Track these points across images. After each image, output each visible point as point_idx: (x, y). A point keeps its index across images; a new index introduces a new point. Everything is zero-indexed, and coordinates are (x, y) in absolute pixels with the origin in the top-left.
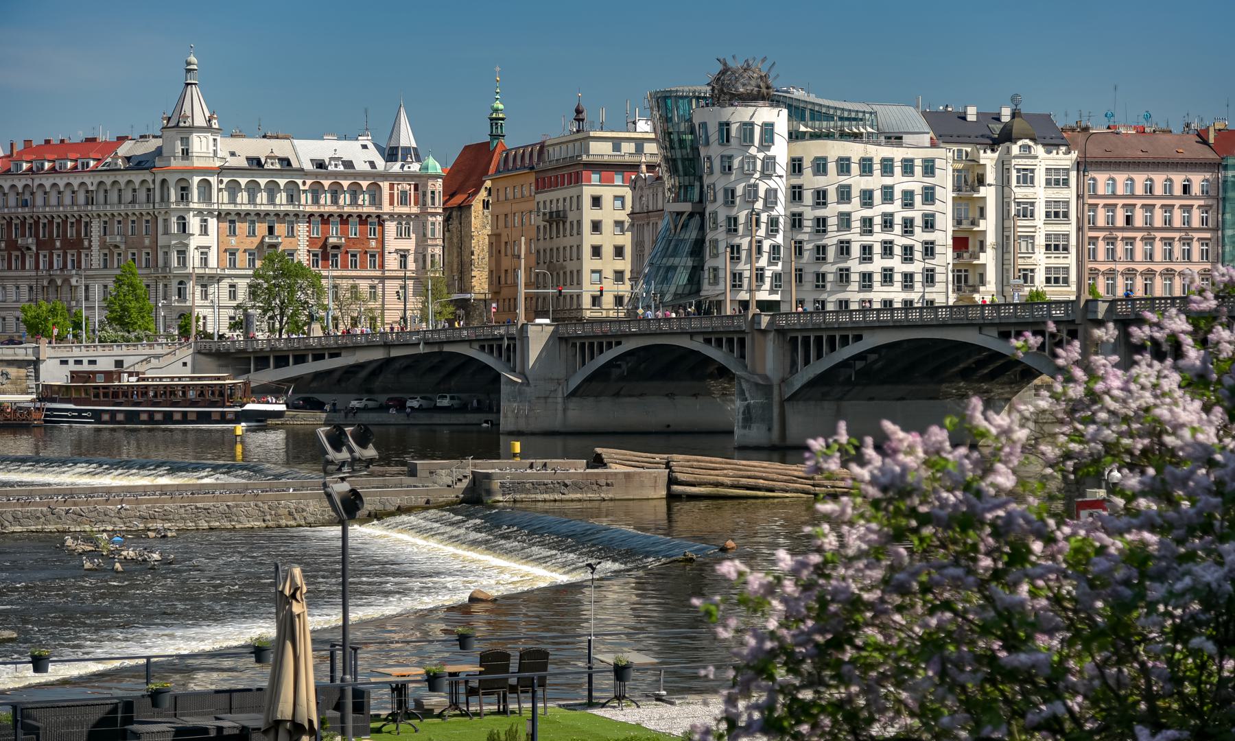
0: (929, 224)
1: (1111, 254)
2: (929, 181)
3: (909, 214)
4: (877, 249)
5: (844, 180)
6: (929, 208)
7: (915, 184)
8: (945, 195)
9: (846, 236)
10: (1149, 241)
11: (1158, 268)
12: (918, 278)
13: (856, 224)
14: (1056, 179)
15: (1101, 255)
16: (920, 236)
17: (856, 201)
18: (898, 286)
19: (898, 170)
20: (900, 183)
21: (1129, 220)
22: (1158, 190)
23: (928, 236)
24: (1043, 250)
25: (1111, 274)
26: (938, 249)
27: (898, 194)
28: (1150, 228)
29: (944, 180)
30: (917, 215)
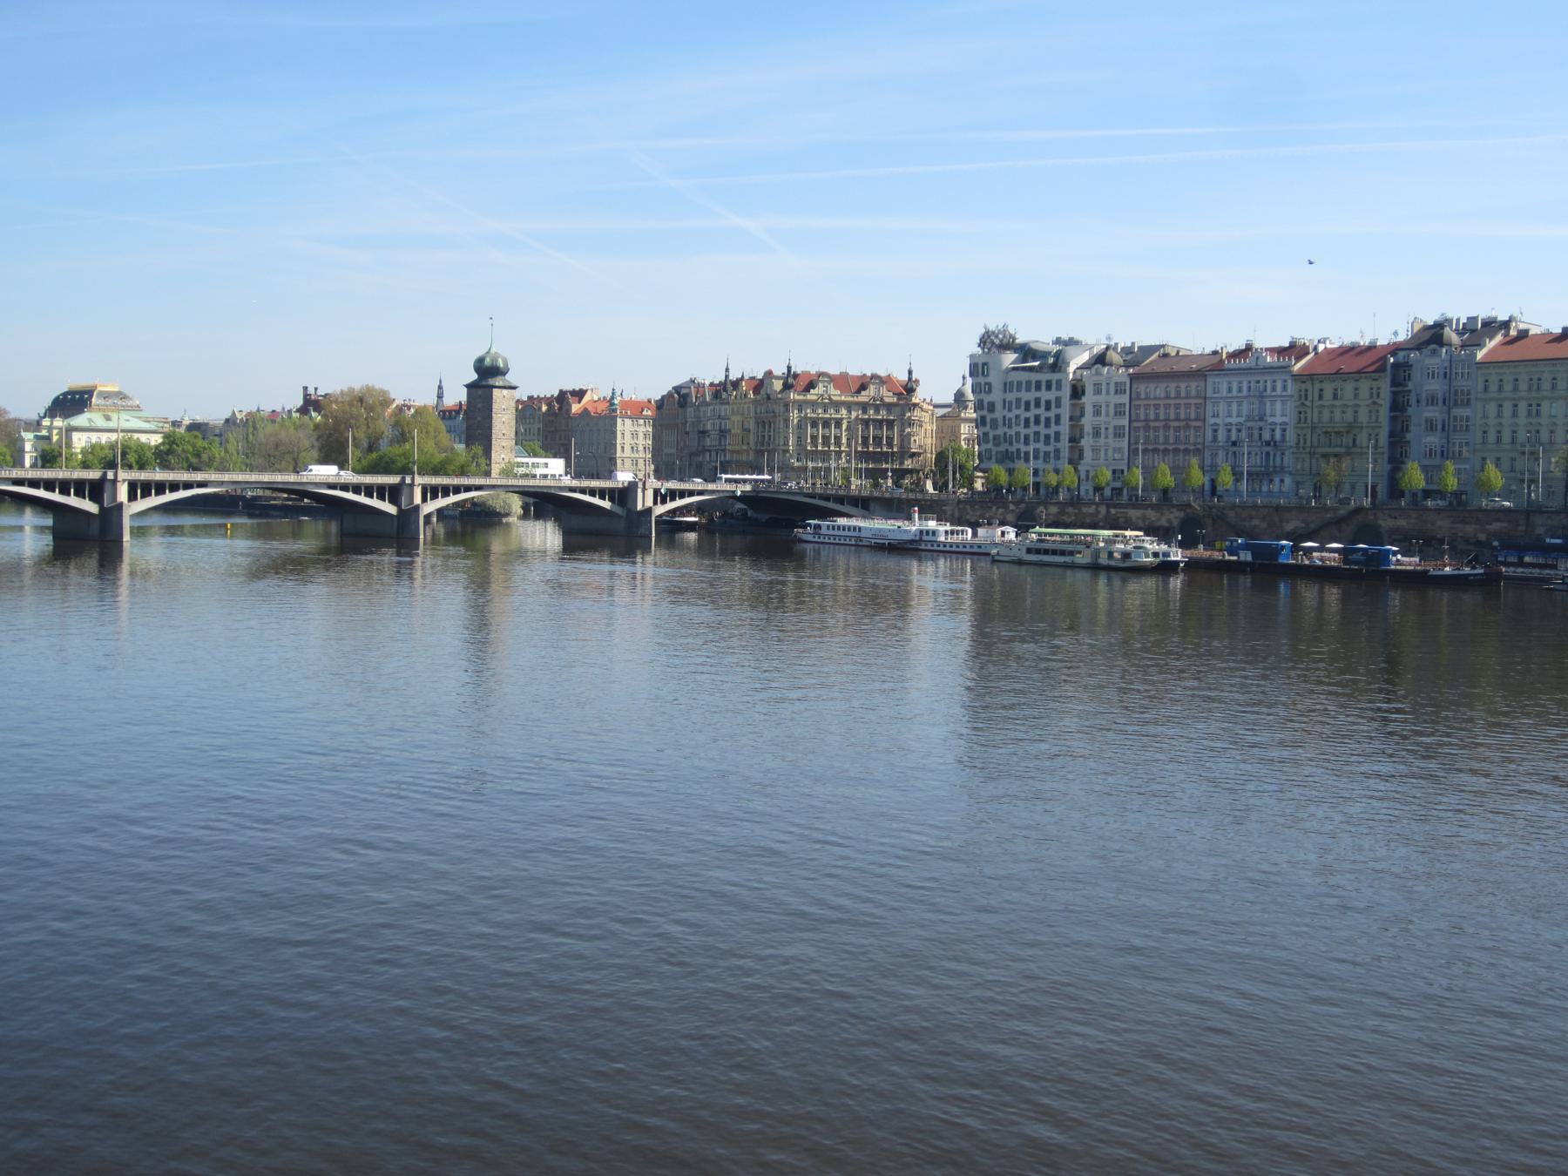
0: (1058, 418)
1: (1166, 438)
2: (1058, 394)
6: (1059, 411)
11: (1171, 448)
16: (1054, 428)
19: (1044, 387)
20: (1045, 395)
24: (1111, 436)
26: (1062, 437)
27: (1043, 403)
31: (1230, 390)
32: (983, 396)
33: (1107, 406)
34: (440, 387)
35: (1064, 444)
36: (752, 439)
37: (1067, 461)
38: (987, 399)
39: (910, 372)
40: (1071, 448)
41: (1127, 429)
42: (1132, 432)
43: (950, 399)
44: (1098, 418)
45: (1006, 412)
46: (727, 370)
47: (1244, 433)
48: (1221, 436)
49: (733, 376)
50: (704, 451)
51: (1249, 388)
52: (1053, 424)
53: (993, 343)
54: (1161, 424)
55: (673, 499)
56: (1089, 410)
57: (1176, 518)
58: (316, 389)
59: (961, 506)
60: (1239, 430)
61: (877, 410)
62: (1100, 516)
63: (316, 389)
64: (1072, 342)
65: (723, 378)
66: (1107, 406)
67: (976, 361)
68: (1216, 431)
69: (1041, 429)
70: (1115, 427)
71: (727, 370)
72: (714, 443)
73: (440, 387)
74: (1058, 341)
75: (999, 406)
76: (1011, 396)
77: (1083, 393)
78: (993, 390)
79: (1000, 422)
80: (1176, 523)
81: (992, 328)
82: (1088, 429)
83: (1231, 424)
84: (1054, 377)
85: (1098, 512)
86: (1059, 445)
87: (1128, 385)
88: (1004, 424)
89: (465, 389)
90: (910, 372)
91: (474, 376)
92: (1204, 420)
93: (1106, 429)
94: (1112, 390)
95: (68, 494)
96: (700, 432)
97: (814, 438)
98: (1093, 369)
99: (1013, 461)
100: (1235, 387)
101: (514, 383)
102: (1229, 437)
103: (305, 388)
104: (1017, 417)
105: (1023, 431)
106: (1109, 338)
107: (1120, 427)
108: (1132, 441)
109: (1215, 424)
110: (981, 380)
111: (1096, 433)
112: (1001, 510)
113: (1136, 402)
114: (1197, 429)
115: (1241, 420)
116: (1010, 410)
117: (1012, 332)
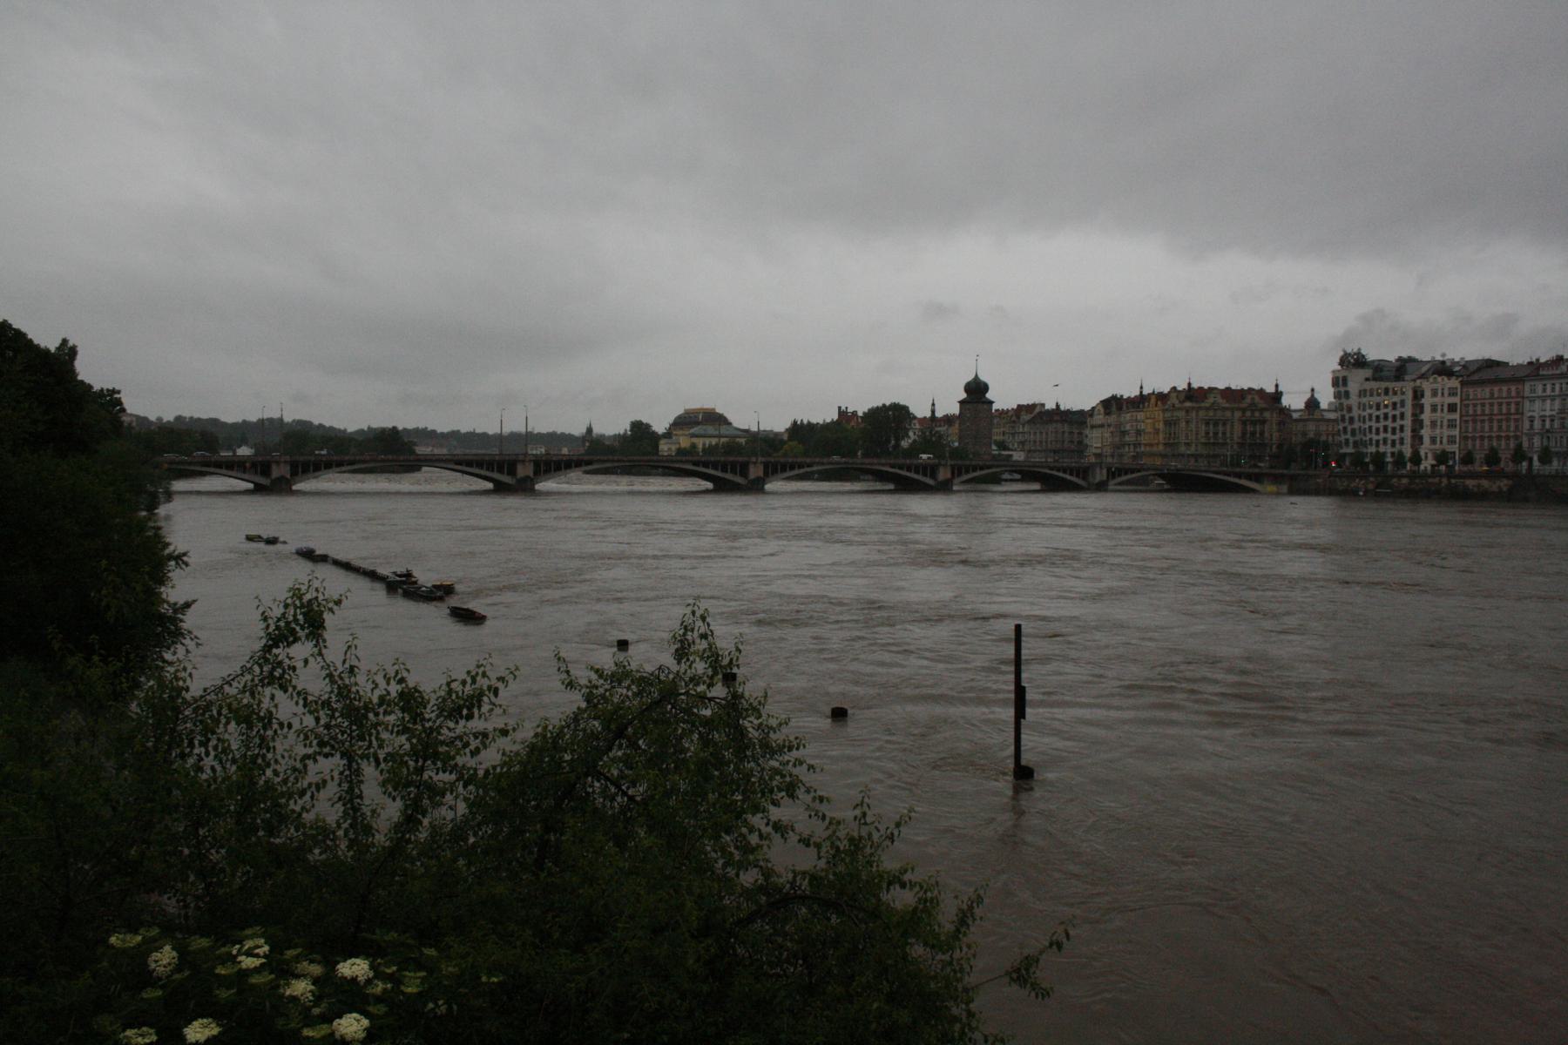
0: (1402, 416)
3: (1394, 413)
4: (1381, 430)
5: (1371, 399)
6: (1403, 410)
7: (1396, 399)
8: (1409, 403)
9: (1377, 425)
10: (1491, 421)
11: (1494, 435)
12: (1397, 442)
13: (1374, 418)
14: (1452, 393)
15: (1487, 428)
16: (1399, 422)
17: (1374, 408)
18: (1389, 446)
21: (1483, 411)
22: (1513, 394)
23: (1402, 423)
24: (1445, 427)
25: (1490, 438)
26: (1405, 428)
28: (1509, 413)
29: (1410, 394)
30: (1397, 413)
31: (1544, 390)
32: (1343, 400)
33: (1442, 406)
34: (933, 405)
35: (1408, 434)
36: (1161, 436)
37: (1409, 446)
38: (1345, 402)
39: (1277, 386)
40: (1413, 437)
41: (1458, 422)
42: (1463, 424)
43: (1302, 406)
44: (1434, 415)
45: (1360, 412)
46: (1141, 388)
47: (1556, 424)
48: (1537, 424)
49: (1145, 392)
50: (1124, 445)
51: (1561, 388)
52: (1398, 420)
53: (1349, 362)
54: (1486, 418)
55: (1120, 475)
56: (1427, 409)
57: (1506, 485)
58: (847, 408)
59: (1332, 479)
60: (1552, 420)
61: (1253, 411)
62: (1443, 485)
63: (847, 408)
64: (1411, 360)
65: (1138, 393)
66: (1442, 406)
67: (1337, 375)
68: (1532, 421)
69: (1389, 423)
70: (1449, 420)
71: (1141, 388)
72: (1132, 439)
73: (933, 405)
74: (1400, 359)
75: (1355, 408)
76: (1364, 400)
77: (1422, 396)
78: (1351, 396)
79: (1356, 419)
80: (1505, 489)
81: (1349, 351)
82: (1427, 422)
83: (1545, 416)
84: (1397, 385)
85: (1441, 482)
86: (1403, 435)
87: (1459, 390)
88: (1359, 420)
89: (958, 405)
90: (1277, 386)
91: (964, 395)
92: (1522, 414)
93: (1442, 422)
94: (1446, 392)
95: (726, 472)
96: (1123, 432)
97: (1207, 433)
98: (1431, 380)
99: (1366, 447)
100: (1549, 387)
101: (993, 400)
102: (1543, 425)
103: (840, 408)
104: (1370, 415)
105: (1374, 425)
106: (1443, 355)
107: (1452, 420)
108: (1463, 430)
109: (1531, 417)
110: (1342, 389)
111: (1433, 424)
112: (1363, 482)
113: (1466, 402)
114: (1516, 420)
115: (1554, 413)
116: (1364, 410)
117: (1364, 353)
